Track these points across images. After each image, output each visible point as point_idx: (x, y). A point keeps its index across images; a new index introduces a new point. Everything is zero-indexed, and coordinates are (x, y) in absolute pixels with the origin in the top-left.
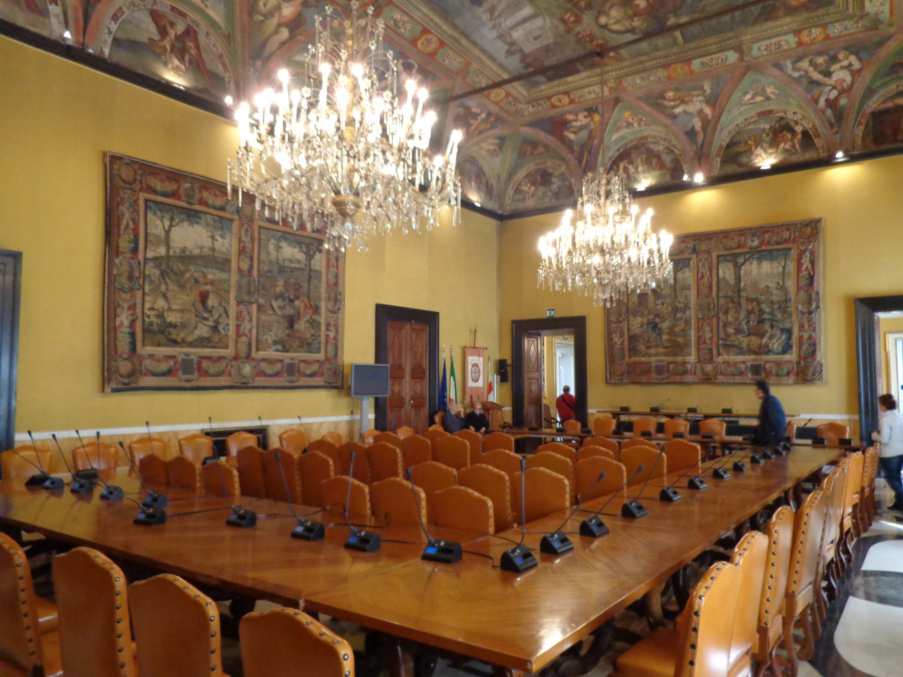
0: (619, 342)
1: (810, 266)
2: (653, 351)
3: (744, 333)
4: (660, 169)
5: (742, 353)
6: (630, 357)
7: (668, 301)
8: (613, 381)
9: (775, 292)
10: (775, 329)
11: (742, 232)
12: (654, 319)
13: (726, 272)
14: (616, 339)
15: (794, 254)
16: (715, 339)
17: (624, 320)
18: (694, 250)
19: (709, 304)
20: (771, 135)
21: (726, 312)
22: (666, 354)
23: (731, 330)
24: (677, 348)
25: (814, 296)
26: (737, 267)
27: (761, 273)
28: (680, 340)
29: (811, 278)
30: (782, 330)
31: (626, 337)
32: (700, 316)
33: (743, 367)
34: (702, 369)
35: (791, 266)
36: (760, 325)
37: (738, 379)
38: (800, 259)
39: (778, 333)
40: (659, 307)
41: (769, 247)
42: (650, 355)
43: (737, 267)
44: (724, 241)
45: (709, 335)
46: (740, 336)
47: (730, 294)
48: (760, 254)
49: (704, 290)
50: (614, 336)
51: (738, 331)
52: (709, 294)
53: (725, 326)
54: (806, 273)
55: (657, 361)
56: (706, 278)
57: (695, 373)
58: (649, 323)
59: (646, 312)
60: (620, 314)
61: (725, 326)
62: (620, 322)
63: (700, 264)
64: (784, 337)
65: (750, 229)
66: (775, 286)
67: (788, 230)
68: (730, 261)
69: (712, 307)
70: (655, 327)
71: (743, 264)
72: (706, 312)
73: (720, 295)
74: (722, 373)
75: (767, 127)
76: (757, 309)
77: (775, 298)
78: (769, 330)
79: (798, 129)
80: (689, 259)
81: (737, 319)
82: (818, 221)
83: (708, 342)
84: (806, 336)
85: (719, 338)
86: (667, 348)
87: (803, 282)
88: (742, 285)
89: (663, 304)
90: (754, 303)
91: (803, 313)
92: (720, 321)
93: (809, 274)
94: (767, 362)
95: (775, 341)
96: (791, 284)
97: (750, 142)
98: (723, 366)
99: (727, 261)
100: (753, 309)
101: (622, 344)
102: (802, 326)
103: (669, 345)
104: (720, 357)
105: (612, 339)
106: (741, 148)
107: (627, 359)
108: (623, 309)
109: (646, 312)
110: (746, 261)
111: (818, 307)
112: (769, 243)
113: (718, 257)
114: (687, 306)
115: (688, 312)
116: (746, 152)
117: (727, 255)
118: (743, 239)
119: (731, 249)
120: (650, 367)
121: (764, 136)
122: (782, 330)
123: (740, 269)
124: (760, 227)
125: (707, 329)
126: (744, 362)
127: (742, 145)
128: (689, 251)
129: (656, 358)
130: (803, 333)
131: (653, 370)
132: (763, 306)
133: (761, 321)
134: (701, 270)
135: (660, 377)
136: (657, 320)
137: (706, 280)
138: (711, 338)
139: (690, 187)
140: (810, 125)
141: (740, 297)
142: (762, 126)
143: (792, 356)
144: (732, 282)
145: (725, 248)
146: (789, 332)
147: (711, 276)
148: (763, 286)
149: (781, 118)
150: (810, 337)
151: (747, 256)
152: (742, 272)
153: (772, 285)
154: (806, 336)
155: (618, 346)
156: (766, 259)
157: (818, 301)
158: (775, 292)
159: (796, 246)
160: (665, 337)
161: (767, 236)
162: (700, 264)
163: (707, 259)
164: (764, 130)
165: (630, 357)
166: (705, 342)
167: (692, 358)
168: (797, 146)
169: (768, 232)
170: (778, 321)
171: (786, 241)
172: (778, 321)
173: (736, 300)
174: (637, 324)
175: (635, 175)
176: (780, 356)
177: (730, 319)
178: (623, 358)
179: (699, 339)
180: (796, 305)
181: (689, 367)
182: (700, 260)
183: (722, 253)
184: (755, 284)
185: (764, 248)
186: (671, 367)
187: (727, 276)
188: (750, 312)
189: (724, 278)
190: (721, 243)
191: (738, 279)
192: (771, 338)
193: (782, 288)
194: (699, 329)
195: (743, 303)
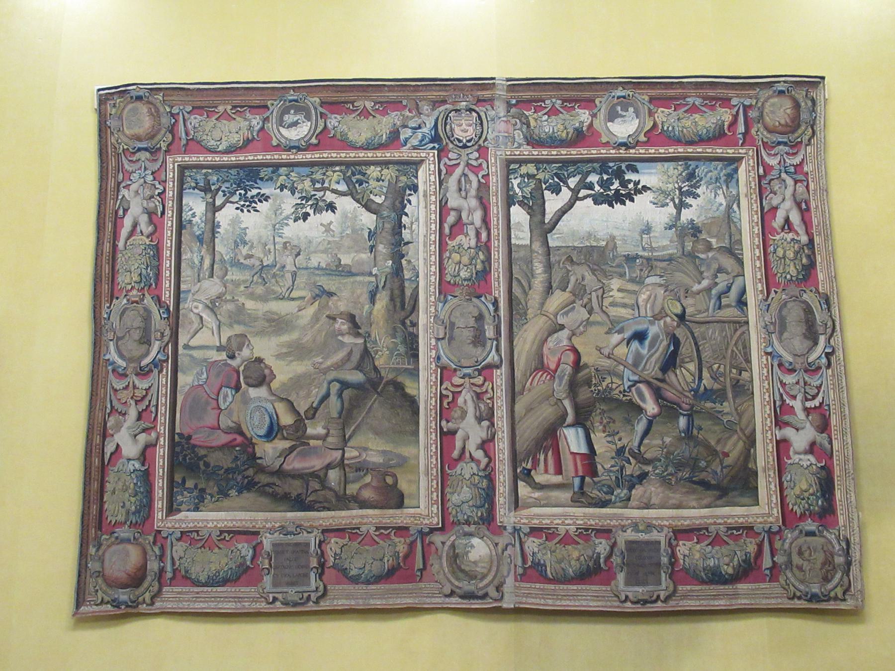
0: (130, 449)
1: (795, 218)
6: (172, 509)
11: (580, 92)
14: (126, 441)
17: (157, 364)
32: (444, 360)
34: (455, 557)
37: (588, 597)
62: (143, 373)
69: (490, 333)
84: (800, 439)
120: (257, 549)
126: (605, 532)
130: (789, 432)
134: (454, 201)
137: (468, 240)
138: (486, 445)
145: (534, 141)
147: (486, 221)
150: (812, 448)
154: (800, 439)
163: (476, 169)
165: (172, 509)
182: (450, 169)
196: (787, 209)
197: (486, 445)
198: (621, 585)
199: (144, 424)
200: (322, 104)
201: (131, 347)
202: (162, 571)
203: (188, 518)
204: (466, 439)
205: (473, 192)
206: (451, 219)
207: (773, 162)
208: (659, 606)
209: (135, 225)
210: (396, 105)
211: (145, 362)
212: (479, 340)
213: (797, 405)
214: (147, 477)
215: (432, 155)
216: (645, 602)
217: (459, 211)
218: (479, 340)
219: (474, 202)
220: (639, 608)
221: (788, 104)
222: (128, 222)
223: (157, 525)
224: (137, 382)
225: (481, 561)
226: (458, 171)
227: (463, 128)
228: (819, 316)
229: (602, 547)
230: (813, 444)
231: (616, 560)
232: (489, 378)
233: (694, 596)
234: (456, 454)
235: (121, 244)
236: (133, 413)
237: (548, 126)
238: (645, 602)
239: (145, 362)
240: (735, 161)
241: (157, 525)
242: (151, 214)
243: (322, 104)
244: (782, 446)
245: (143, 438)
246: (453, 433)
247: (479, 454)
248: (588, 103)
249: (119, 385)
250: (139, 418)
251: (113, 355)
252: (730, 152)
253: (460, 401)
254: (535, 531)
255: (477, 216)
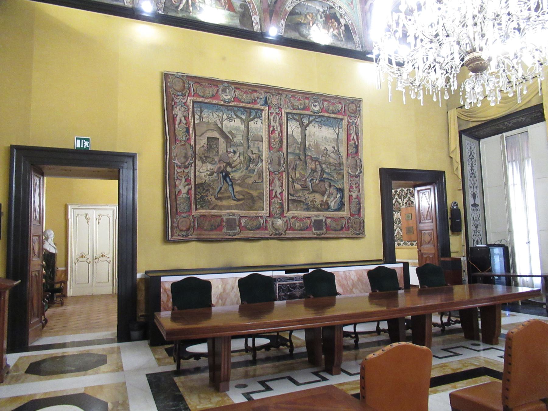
0: (184, 191)
1: (355, 137)
2: (225, 203)
3: (309, 190)
4: (228, 9)
5: (308, 209)
6: (196, 209)
7: (241, 149)
8: (175, 238)
9: (332, 155)
10: (332, 188)
12: (226, 167)
13: (294, 129)
15: (344, 123)
16: (285, 193)
18: (266, 102)
19: (279, 159)
20: (324, 19)
21: (295, 169)
22: (238, 208)
23: (298, 186)
24: (251, 201)
25: (358, 162)
26: (304, 127)
27: (321, 135)
28: (255, 193)
29: (357, 147)
30: (337, 189)
31: (193, 183)
32: (271, 170)
33: (308, 221)
34: (273, 224)
35: (343, 136)
36: (322, 183)
38: (348, 130)
39: (335, 192)
40: (231, 155)
41: (327, 115)
42: (220, 208)
43: (304, 127)
44: (292, 99)
45: (279, 191)
46: (306, 192)
47: (298, 152)
48: (323, 119)
49: (275, 145)
50: (177, 182)
51: (305, 188)
52: (280, 149)
53: (293, 182)
54: (353, 142)
55: (229, 214)
56: (277, 132)
57: (266, 229)
58: (220, 171)
59: (217, 159)
60: (186, 157)
61: (293, 182)
62: (186, 167)
63: (272, 118)
64: (339, 195)
65: (313, 94)
66: (332, 149)
67: (340, 103)
68: (297, 120)
69: (282, 162)
70: (226, 176)
71: (308, 125)
72: (277, 167)
73: (289, 151)
74: (292, 229)
75: (321, 10)
76: (319, 168)
77: (332, 160)
78: (328, 188)
79: (343, 21)
80: (262, 110)
81: (302, 176)
82: (359, 101)
83: (279, 196)
84: (354, 195)
85: (288, 193)
86: (238, 200)
87: (352, 150)
88: (307, 144)
89: (235, 152)
90: (317, 163)
91: (351, 176)
92: (290, 176)
93: (355, 143)
94: (327, 217)
95: (332, 198)
96: (343, 150)
97: (308, 16)
98: (292, 221)
99: (294, 119)
100: (316, 167)
101: (188, 192)
102: (351, 187)
103: (241, 197)
104: (290, 212)
105: (175, 186)
106: (302, 20)
107: (193, 211)
108: (190, 152)
109: (217, 159)
110: (310, 123)
111: (361, 172)
112: (327, 111)
113: (287, 113)
114: (260, 157)
115: (260, 165)
116: (305, 24)
117: (295, 114)
118: (307, 102)
119: (298, 109)
120: (222, 220)
121: (319, 16)
122: (337, 189)
123: (305, 130)
124: (321, 95)
125: (278, 183)
126: (309, 218)
127: (302, 17)
128: (262, 102)
129: (227, 210)
130: (352, 193)
131: (224, 224)
132: (324, 166)
133: (322, 180)
134: (272, 124)
135: (231, 232)
136: (229, 169)
138: (281, 193)
139: (260, 37)
140: (350, 22)
141: (305, 155)
142: (317, 8)
143: (345, 213)
144: (299, 141)
146: (342, 191)
148: (323, 148)
149: (331, 8)
150: (357, 197)
151: (311, 119)
152: (307, 132)
153: (330, 148)
154: (354, 195)
155: (183, 195)
156: (325, 125)
157: (361, 167)
158: (332, 155)
159: (345, 117)
160: (237, 189)
161: (325, 104)
162: (272, 118)
164: (319, 11)
166: (276, 196)
167: (264, 212)
168: (342, 36)
169: (326, 101)
170: (334, 181)
171: (339, 112)
172: (334, 181)
173: (303, 158)
174: (204, 171)
175: (201, 5)
176: (336, 213)
177: (298, 176)
178: (189, 210)
179: (271, 191)
180: (346, 170)
181: (261, 221)
182: (272, 114)
183: (291, 111)
184: (317, 146)
185: (323, 114)
186: (243, 221)
187: (295, 134)
188: (314, 171)
189: (292, 135)
190: (290, 101)
191: (304, 138)
192: (329, 197)
193: (337, 152)
194: (271, 183)
195: (309, 161)
196: (353, 135)
197: (281, 193)
198: (314, 231)
199: (186, 183)
200: (235, 88)
201: (183, 160)
202: (194, 226)
203: (202, 211)
204: (276, 192)
205: (277, 121)
206: (271, 129)
207: (351, 121)
208: (323, 236)
209: (181, 120)
210: (256, 91)
211: (187, 164)
212: (279, 164)
213: (354, 186)
214: (190, 199)
215: (266, 108)
216: (319, 235)
217: (274, 127)
218: (279, 164)
219: (278, 124)
220: (318, 237)
221: (354, 105)
222: (178, 118)
223: (193, 213)
224: (185, 170)
225: (280, 225)
226: (274, 114)
227: (274, 101)
228: (358, 164)
229: (308, 221)
230: (357, 196)
231: (312, 224)
232: (282, 175)
233: (332, 234)
234: (273, 196)
235: (177, 126)
236: (184, 180)
237: (296, 103)
238: (319, 235)
239: (187, 164)
240: (342, 119)
241: (193, 213)
242: (185, 117)
243: (235, 88)
244: (351, 196)
245: (187, 187)
246: (273, 190)
247: (279, 196)
248: (308, 98)
249: (179, 171)
250: (186, 181)
251: (176, 162)
252: (340, 117)
253: (274, 181)
254: (293, 217)
255: (279, 128)
